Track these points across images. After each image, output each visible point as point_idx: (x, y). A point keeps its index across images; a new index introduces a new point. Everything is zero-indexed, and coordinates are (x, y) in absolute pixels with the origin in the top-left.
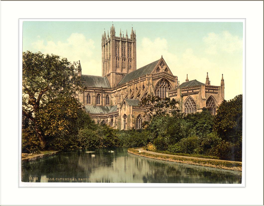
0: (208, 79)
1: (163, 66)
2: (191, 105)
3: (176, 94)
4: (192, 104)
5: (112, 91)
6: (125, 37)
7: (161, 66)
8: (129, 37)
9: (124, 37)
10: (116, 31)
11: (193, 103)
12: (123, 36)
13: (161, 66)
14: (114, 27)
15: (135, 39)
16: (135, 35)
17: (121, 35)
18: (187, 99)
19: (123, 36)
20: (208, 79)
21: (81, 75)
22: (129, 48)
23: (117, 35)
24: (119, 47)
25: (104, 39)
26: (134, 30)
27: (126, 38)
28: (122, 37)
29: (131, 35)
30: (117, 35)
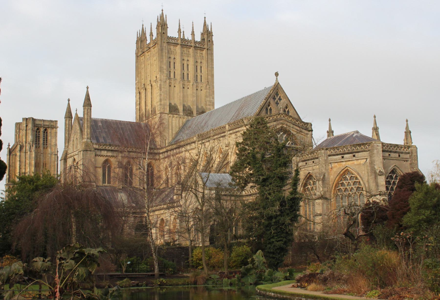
0: (376, 129)
1: (279, 102)
2: (350, 187)
3: (316, 161)
4: (354, 184)
5: (159, 154)
6: (188, 36)
7: (276, 101)
8: (198, 38)
9: (186, 38)
10: (169, 23)
11: (355, 182)
12: (183, 34)
13: (276, 101)
14: (165, 17)
15: (211, 42)
16: (212, 32)
17: (181, 32)
18: (342, 174)
19: (183, 34)
20: (376, 129)
21: (91, 118)
22: (197, 62)
23: (172, 32)
24: (174, 58)
25: (141, 39)
26: (208, 23)
27: (190, 38)
28: (182, 37)
29: (202, 34)
30: (172, 32)
